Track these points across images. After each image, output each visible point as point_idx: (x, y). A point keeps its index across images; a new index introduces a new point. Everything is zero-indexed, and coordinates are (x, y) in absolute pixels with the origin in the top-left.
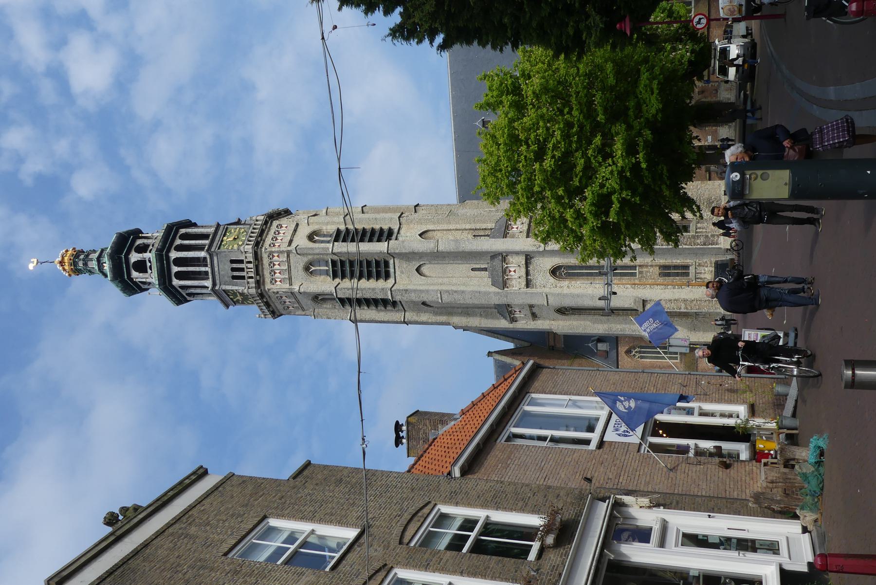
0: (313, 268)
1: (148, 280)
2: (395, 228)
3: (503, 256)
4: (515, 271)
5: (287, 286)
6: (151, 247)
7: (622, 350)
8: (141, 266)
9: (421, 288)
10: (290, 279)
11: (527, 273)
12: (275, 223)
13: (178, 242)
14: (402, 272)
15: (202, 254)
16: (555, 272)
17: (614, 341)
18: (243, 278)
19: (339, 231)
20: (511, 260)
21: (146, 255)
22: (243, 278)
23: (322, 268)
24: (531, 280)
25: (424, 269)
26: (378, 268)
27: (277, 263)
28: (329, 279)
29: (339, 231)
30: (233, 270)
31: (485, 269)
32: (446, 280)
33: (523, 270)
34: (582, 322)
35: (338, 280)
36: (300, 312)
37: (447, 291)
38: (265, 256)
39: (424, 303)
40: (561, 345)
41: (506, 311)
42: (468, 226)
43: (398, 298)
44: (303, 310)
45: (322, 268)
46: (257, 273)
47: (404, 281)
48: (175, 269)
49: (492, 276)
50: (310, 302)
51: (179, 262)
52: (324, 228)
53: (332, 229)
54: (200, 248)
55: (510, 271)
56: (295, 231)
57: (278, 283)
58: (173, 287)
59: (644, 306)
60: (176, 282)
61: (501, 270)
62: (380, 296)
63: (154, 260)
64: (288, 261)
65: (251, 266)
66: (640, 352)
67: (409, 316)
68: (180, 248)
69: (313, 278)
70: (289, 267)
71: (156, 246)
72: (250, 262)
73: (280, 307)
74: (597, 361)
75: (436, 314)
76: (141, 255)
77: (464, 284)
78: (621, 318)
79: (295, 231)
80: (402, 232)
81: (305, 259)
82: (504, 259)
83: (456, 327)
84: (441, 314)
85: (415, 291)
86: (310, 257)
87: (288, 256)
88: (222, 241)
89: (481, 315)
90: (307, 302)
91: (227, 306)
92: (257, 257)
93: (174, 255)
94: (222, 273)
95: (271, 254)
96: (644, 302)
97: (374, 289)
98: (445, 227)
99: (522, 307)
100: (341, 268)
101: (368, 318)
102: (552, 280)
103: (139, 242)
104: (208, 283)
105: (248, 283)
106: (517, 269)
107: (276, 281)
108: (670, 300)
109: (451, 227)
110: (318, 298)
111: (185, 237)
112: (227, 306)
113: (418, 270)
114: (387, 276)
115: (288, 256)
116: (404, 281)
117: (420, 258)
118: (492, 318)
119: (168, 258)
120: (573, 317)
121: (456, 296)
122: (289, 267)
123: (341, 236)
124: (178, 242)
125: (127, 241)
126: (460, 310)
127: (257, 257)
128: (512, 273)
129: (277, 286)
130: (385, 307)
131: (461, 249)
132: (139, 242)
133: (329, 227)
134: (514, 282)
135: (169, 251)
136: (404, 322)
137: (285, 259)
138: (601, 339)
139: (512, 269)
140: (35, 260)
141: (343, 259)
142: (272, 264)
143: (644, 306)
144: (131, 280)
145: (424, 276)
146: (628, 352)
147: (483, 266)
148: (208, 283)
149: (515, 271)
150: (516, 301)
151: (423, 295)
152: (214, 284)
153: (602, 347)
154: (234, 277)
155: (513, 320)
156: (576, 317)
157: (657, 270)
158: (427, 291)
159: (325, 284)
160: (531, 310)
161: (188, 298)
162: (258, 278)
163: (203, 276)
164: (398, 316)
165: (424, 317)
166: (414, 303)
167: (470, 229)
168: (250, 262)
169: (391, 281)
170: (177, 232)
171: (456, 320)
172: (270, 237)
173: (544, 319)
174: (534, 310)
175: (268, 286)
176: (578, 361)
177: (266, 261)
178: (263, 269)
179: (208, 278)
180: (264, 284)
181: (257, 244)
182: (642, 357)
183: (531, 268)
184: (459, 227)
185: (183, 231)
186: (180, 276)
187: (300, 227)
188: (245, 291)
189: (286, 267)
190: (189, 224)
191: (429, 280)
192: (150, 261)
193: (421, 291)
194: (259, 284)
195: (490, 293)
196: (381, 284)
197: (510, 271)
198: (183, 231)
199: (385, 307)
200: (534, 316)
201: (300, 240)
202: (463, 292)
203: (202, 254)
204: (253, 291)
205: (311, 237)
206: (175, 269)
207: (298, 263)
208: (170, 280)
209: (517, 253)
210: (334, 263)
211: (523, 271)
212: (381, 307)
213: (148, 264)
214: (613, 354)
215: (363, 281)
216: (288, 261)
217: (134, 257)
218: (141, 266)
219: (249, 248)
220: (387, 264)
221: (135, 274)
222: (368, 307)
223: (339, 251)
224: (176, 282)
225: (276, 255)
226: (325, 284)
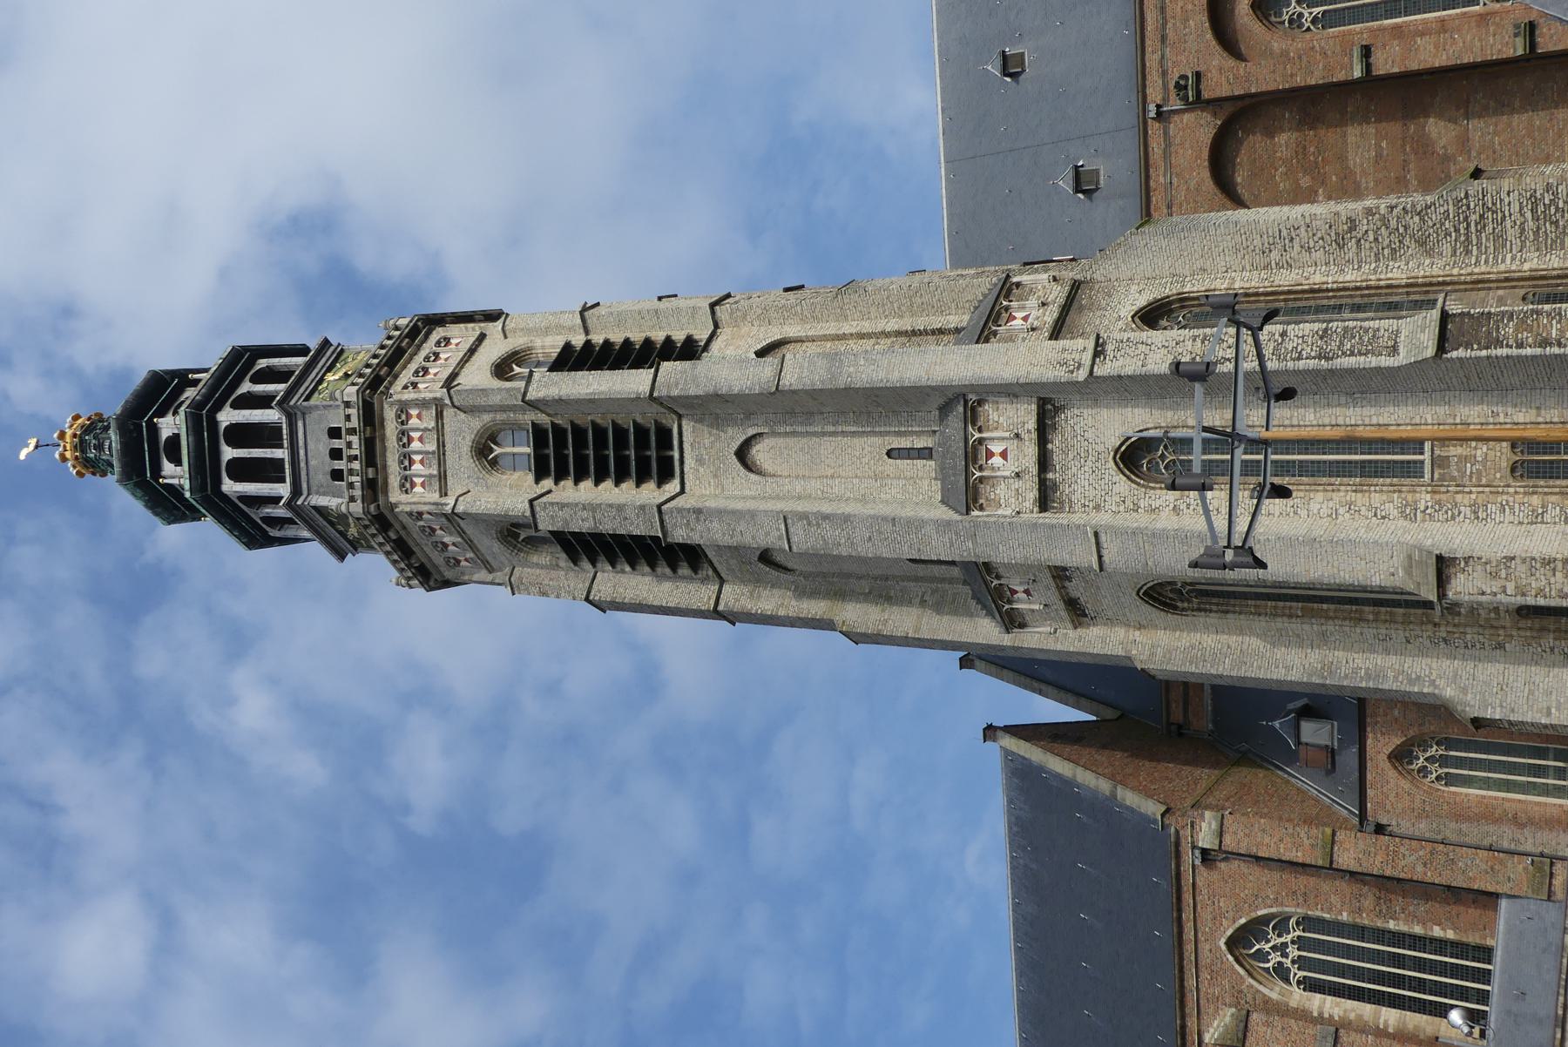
0: (498, 450)
2: (702, 335)
3: (966, 403)
4: (1004, 455)
5: (435, 497)
7: (1380, 746)
9: (739, 505)
10: (442, 477)
11: (1044, 462)
12: (439, 333)
13: (246, 387)
14: (700, 461)
16: (1134, 457)
17: (1353, 711)
19: (568, 347)
20: (993, 416)
23: (516, 450)
24: (1055, 486)
25: (759, 453)
26: (640, 449)
27: (415, 435)
28: (531, 477)
29: (568, 347)
31: (925, 454)
32: (814, 486)
33: (1031, 450)
34: (1234, 640)
35: (548, 483)
36: (482, 575)
37: (804, 516)
38: (390, 414)
39: (766, 557)
40: (1204, 722)
41: (984, 585)
42: (893, 325)
43: (679, 535)
44: (491, 570)
45: (516, 450)
47: (710, 489)
48: (228, 453)
49: (943, 475)
50: (497, 547)
51: (240, 434)
52: (538, 342)
53: (551, 345)
54: (263, 402)
55: (990, 454)
56: (472, 351)
57: (418, 489)
59: (1442, 582)
60: (229, 486)
61: (961, 452)
62: (639, 529)
64: (439, 429)
65: (355, 439)
66: (1444, 761)
67: (734, 596)
69: (495, 478)
70: (441, 445)
72: (352, 431)
73: (437, 558)
74: (1304, 782)
75: (801, 593)
77: (863, 500)
78: (1369, 632)
79: (472, 351)
80: (715, 346)
81: (477, 423)
82: (972, 416)
83: (857, 638)
84: (814, 594)
85: (720, 513)
86: (487, 418)
87: (439, 416)
88: (321, 381)
89: (923, 603)
90: (491, 546)
91: (341, 556)
92: (370, 416)
93: (228, 417)
94: (312, 463)
95: (403, 409)
96: (1443, 566)
97: (620, 508)
98: (831, 328)
99: (1024, 568)
100: (568, 448)
101: (628, 596)
102: (1122, 485)
104: (284, 490)
105: (351, 486)
106: (1012, 446)
107: (413, 485)
108: (1548, 562)
109: (847, 328)
110: (516, 534)
112: (341, 556)
113: (742, 454)
114: (665, 474)
115: (439, 416)
116: (710, 489)
117: (748, 415)
118: (955, 612)
119: (214, 424)
120: (1201, 619)
121: (830, 532)
122: (441, 445)
123: (569, 360)
124: (246, 387)
125: (161, 389)
126: (865, 586)
127: (370, 416)
128: (997, 461)
129: (414, 496)
130: (674, 569)
131: (841, 383)
133: (549, 341)
134: (1001, 491)
135: (218, 407)
136: (716, 614)
137: (432, 424)
138: (1316, 704)
139: (996, 448)
140: (33, 442)
141: (559, 421)
142: (404, 436)
143: (1442, 582)
145: (759, 472)
146: (1400, 757)
147: (920, 443)
148: (284, 490)
149: (1004, 455)
150: (1003, 553)
151: (742, 527)
152: (296, 491)
153: (1315, 733)
155: (1012, 621)
156: (1213, 619)
157: (1503, 455)
158: (753, 514)
159: (511, 492)
160: (1061, 588)
161: (274, 533)
162: (371, 473)
163: (270, 471)
164: (700, 594)
165: (770, 601)
166: (736, 550)
167: (899, 333)
168: (352, 431)
169: (673, 487)
170: (251, 363)
171: (855, 614)
172: (413, 366)
173: (1111, 622)
174: (1076, 588)
175: (395, 496)
176: (1244, 774)
177: (391, 428)
178: (384, 449)
179: (283, 481)
180: (386, 492)
182: (1450, 780)
183: (1055, 445)
184: (867, 327)
185: (263, 363)
186: (241, 470)
187: (486, 343)
188: (343, 508)
189: (432, 447)
191: (770, 486)
193: (737, 515)
194: (374, 488)
195: (922, 523)
196: (649, 494)
197: (990, 454)
198: (263, 363)
199: (674, 569)
200: (1077, 612)
201: (477, 375)
202: (847, 518)
204: (357, 508)
205: (502, 369)
206: (228, 453)
207: (462, 431)
208: (219, 482)
209: (1011, 391)
210: (539, 434)
211: (1028, 454)
212: (684, 570)
214: (1349, 758)
215: (608, 484)
216: (439, 429)
219: (351, 393)
220: (664, 436)
221: (168, 467)
222: (633, 567)
223: (541, 395)
224: (229, 486)
225: (414, 412)
226: (511, 492)
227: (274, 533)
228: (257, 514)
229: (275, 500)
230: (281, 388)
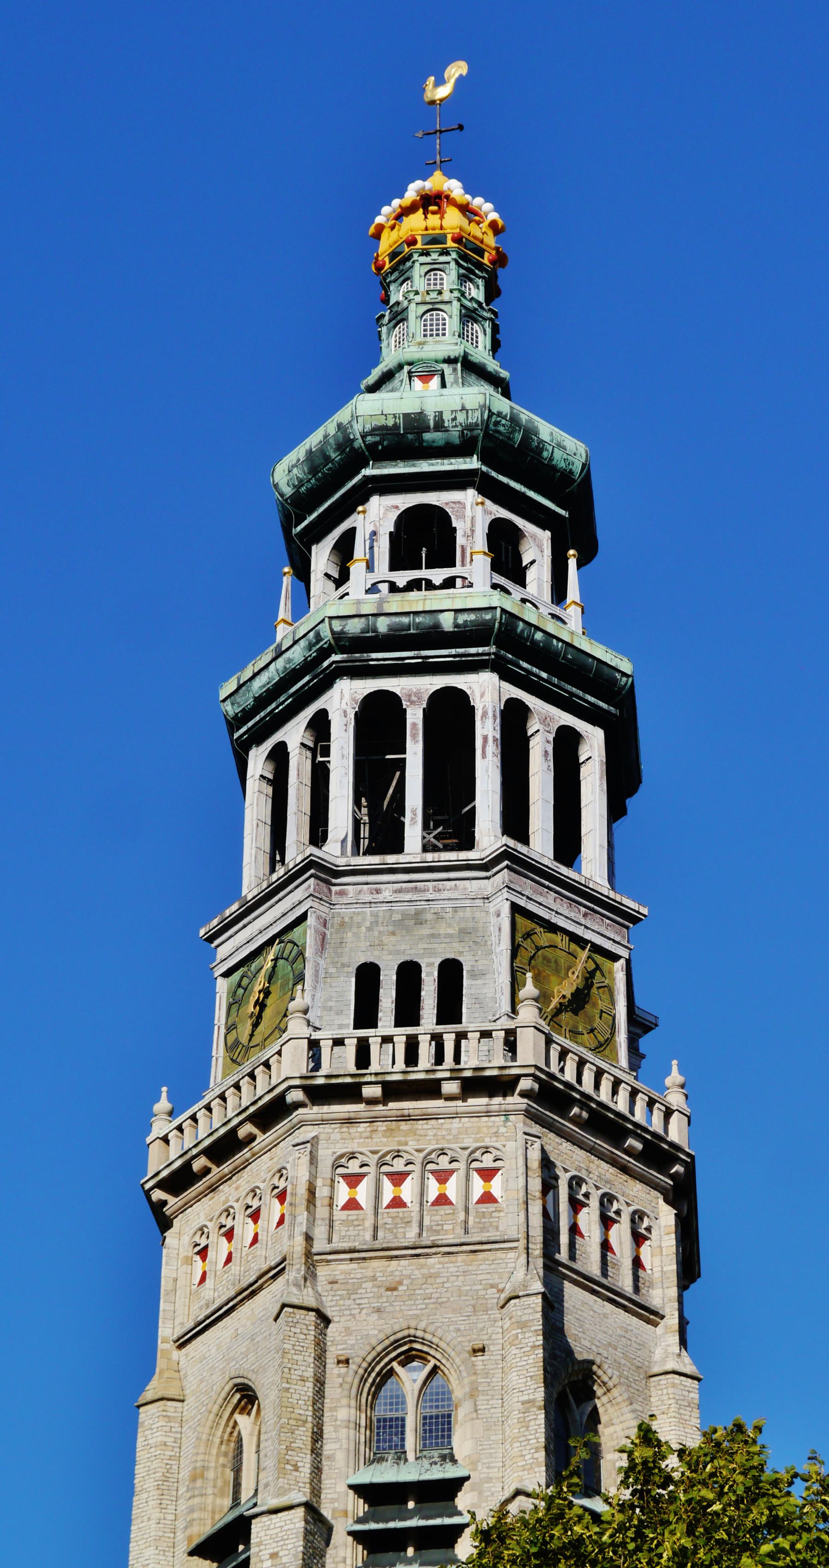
1: (357, 569)
8: (423, 541)
13: (545, 719)
30: (409, 974)
46: (394, 1091)
51: (450, 716)
58: (325, 684)
60: (343, 700)
76: (480, 542)
93: (485, 691)
111: (566, 744)
192: (449, 583)
203: (489, 834)
213: (438, 575)
217: (471, 515)
218: (423, 541)
224: (343, 700)
227: (258, 761)
228: (294, 734)
229: (318, 832)
230: (541, 843)
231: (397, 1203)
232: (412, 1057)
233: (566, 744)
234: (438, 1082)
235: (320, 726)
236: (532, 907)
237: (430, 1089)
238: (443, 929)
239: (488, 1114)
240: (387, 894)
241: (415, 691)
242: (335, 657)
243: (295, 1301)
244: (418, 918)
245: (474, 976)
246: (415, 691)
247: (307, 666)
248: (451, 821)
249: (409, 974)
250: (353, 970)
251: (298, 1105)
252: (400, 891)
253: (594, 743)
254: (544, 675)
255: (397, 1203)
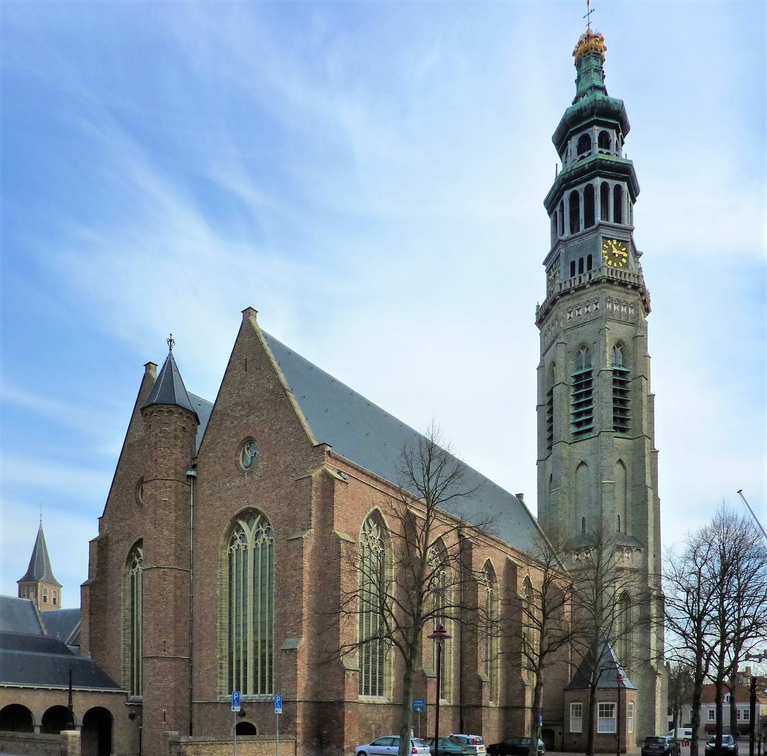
6: (605, 151)
8: (585, 145)
13: (612, 183)
15: (598, 218)
18: (573, 274)
21: (596, 149)
22: (573, 274)
30: (581, 261)
51: (590, 191)
60: (567, 195)
63: (591, 158)
68: (604, 187)
71: (606, 157)
103: (612, 134)
132: (612, 134)
144: (570, 138)
148: (567, 234)
154: (573, 264)
181: (610, 281)
186: (574, 198)
190: (634, 192)
192: (590, 154)
213: (586, 154)
218: (585, 145)
224: (567, 195)
231: (579, 315)
232: (580, 281)
233: (618, 189)
234: (585, 285)
235: (562, 203)
236: (606, 236)
237: (584, 287)
238: (588, 247)
239: (596, 290)
240: (576, 243)
241: (580, 188)
242: (563, 186)
243: (559, 342)
244: (583, 247)
245: (594, 257)
246: (580, 188)
247: (559, 189)
248: (590, 220)
249: (581, 261)
250: (570, 264)
251: (558, 299)
252: (579, 241)
253: (625, 186)
254: (610, 173)
255: (579, 315)
